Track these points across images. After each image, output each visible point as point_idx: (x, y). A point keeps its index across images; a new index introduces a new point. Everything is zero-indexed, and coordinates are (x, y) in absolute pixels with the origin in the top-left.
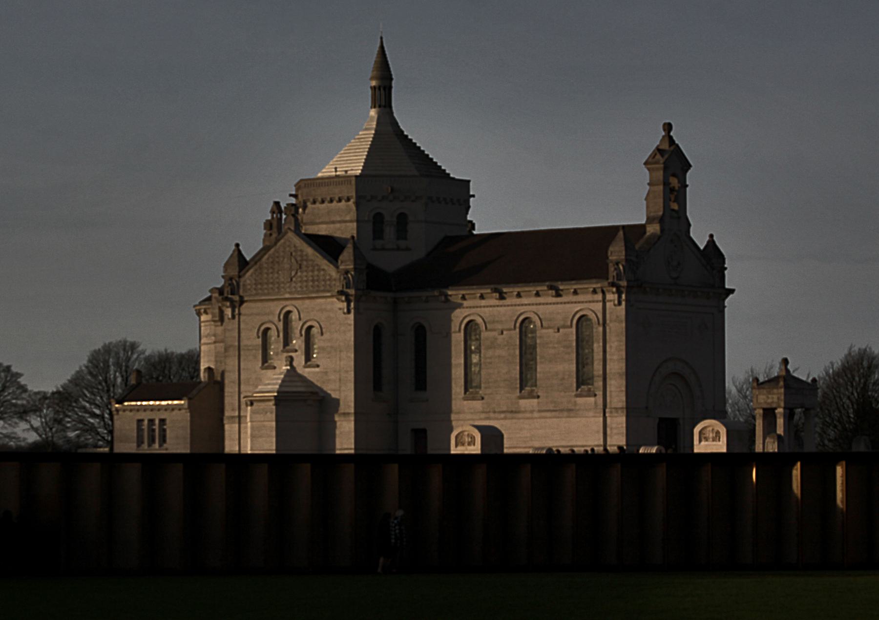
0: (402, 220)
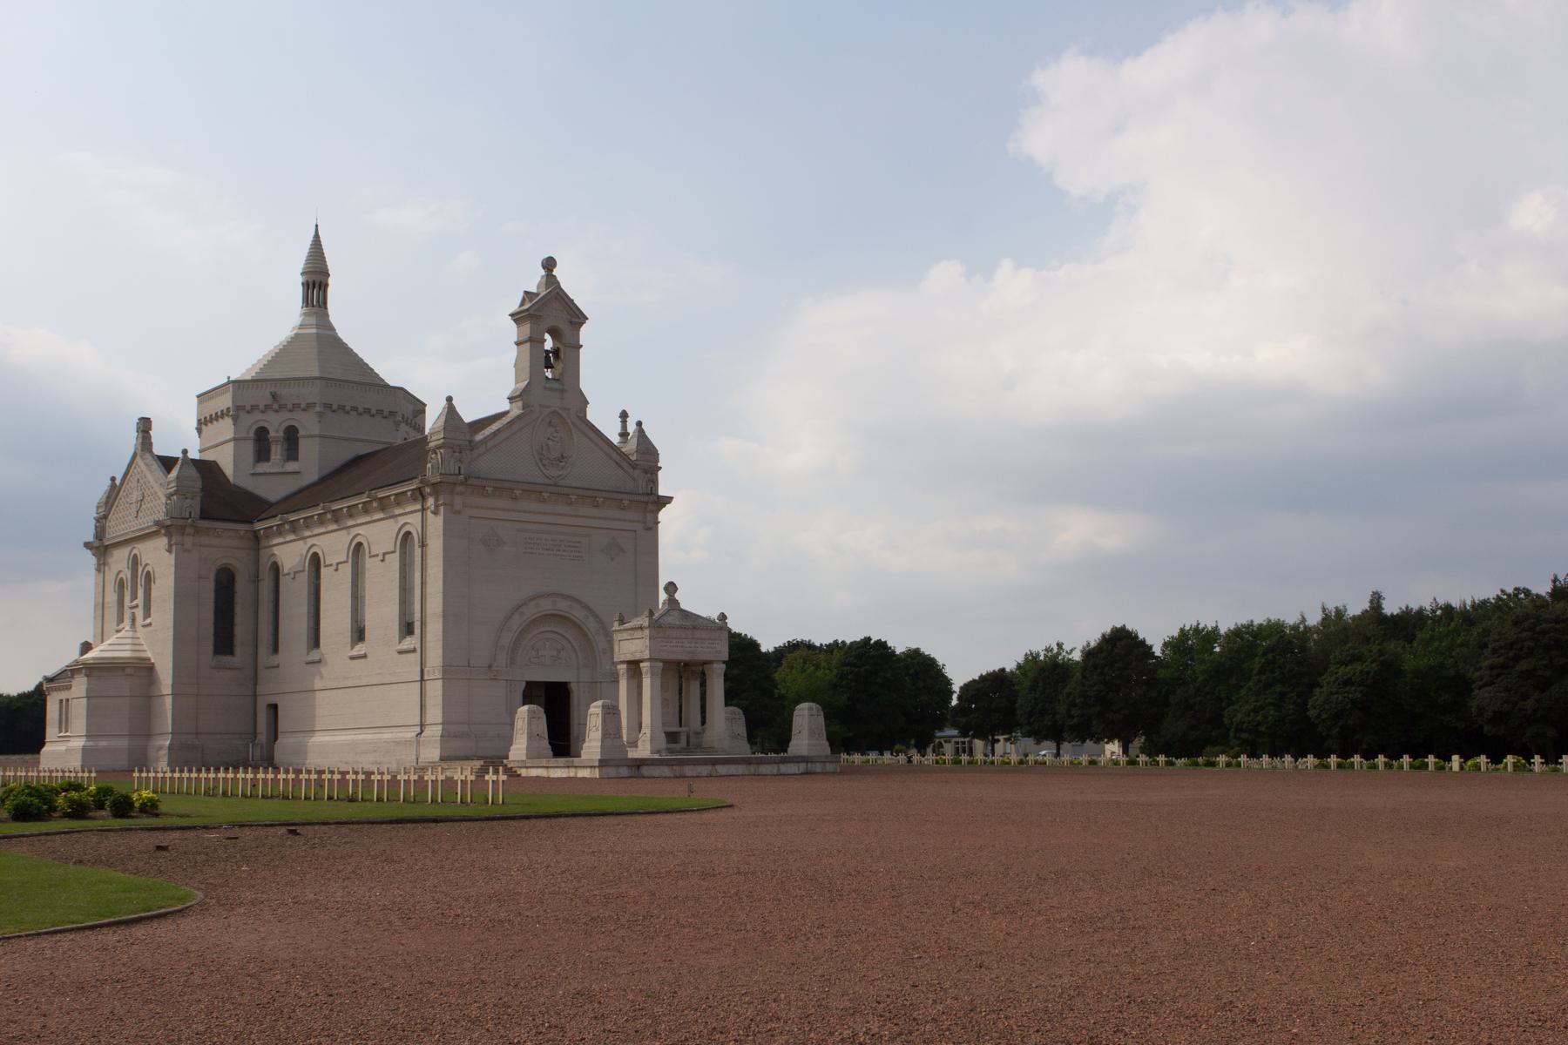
0: (291, 437)
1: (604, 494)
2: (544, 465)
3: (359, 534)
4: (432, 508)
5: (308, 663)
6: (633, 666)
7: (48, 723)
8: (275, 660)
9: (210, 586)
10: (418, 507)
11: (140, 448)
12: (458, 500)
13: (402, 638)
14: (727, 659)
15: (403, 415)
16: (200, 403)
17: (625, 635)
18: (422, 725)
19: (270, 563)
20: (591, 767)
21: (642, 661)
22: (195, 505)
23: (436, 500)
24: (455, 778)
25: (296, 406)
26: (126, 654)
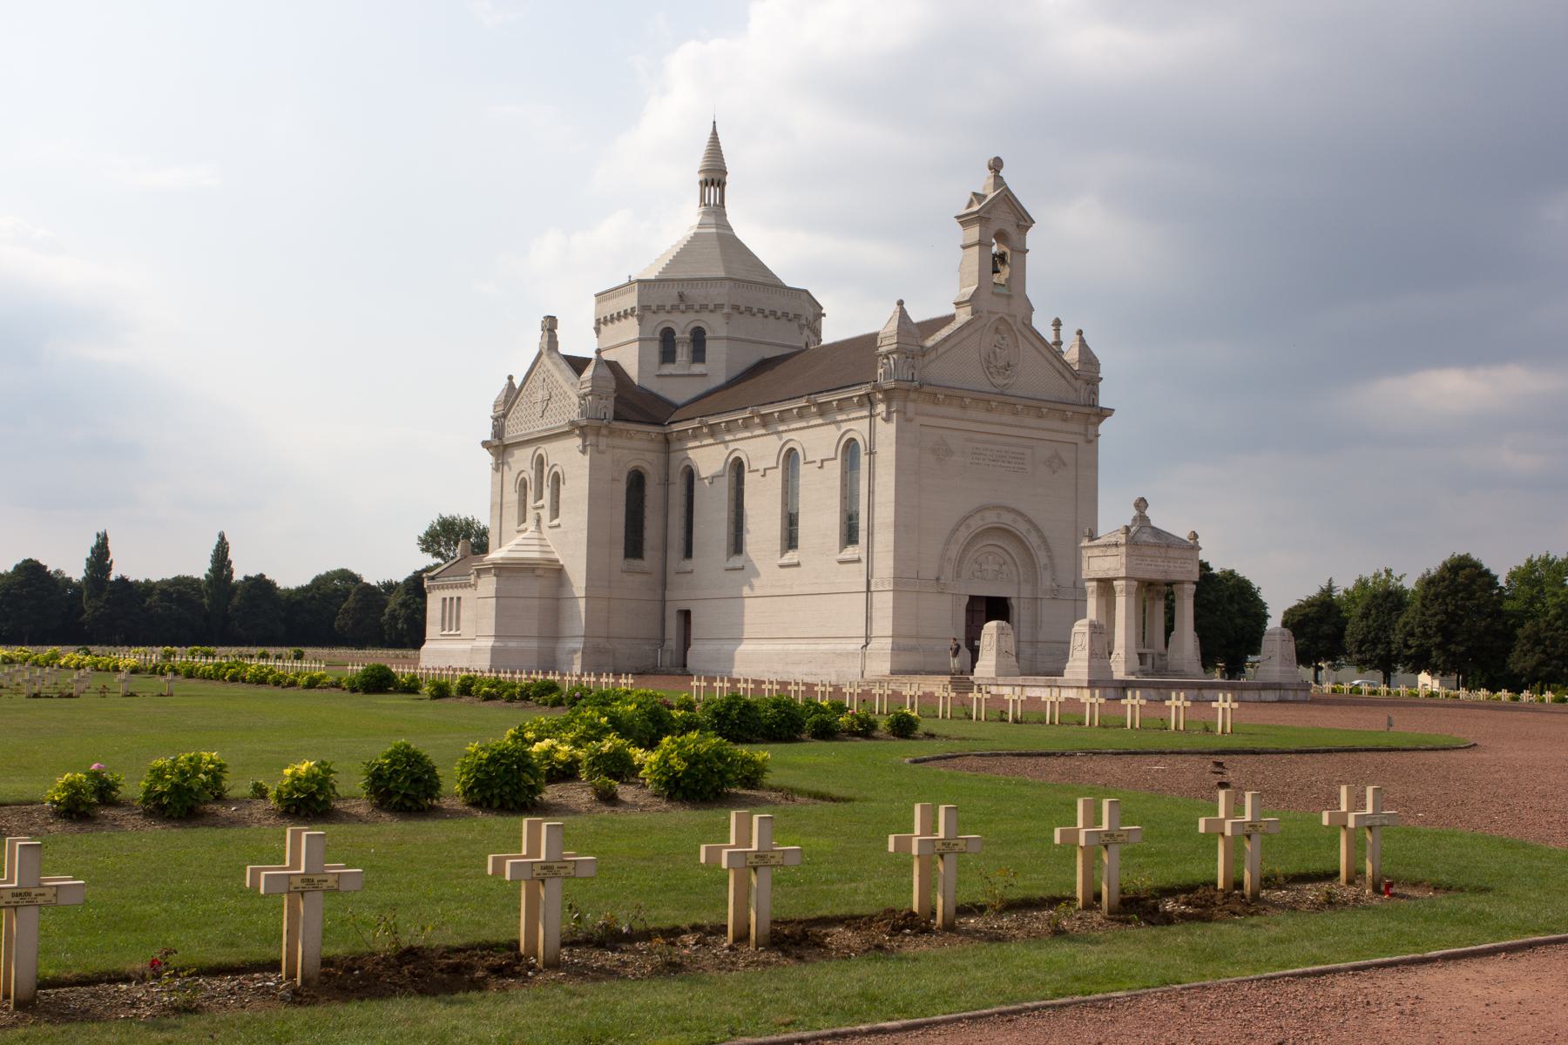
0: (698, 339)
1: (1048, 405)
2: (991, 373)
3: (791, 440)
4: (884, 415)
5: (727, 570)
6: (1102, 584)
7: (428, 621)
8: (687, 565)
9: (622, 487)
10: (866, 413)
11: (546, 347)
12: (911, 407)
13: (843, 547)
14: (1198, 580)
15: (807, 319)
16: (598, 302)
17: (1096, 552)
18: (868, 638)
19: (682, 467)
20: (1078, 687)
21: (1116, 579)
22: (609, 406)
23: (888, 407)
24: (903, 694)
25: (704, 307)
26: (533, 554)
